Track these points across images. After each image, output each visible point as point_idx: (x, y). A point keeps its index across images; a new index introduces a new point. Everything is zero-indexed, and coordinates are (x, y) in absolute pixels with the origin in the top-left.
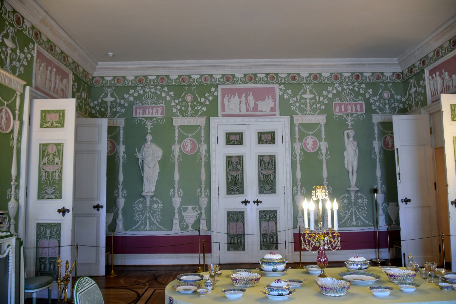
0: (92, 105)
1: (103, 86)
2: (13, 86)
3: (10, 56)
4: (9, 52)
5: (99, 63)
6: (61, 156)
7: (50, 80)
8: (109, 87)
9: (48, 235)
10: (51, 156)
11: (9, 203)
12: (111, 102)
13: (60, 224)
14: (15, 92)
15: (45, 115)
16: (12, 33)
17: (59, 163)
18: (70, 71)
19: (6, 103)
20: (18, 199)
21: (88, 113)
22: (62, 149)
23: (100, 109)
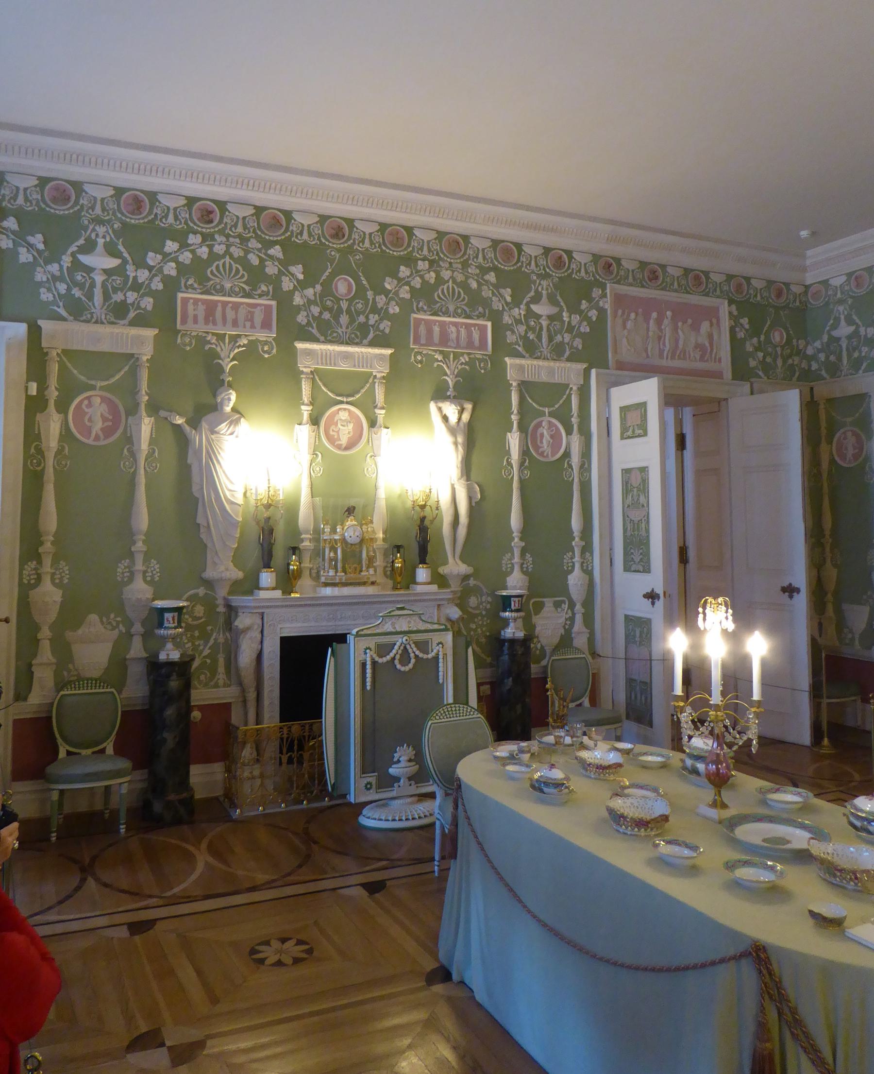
0: (810, 351)
1: (827, 304)
2: (557, 379)
3: (548, 330)
4: (545, 323)
5: (809, 253)
7: (659, 338)
8: (841, 302)
10: (635, 490)
12: (849, 337)
16: (547, 289)
18: (719, 300)
19: (547, 410)
21: (797, 374)
23: (827, 357)
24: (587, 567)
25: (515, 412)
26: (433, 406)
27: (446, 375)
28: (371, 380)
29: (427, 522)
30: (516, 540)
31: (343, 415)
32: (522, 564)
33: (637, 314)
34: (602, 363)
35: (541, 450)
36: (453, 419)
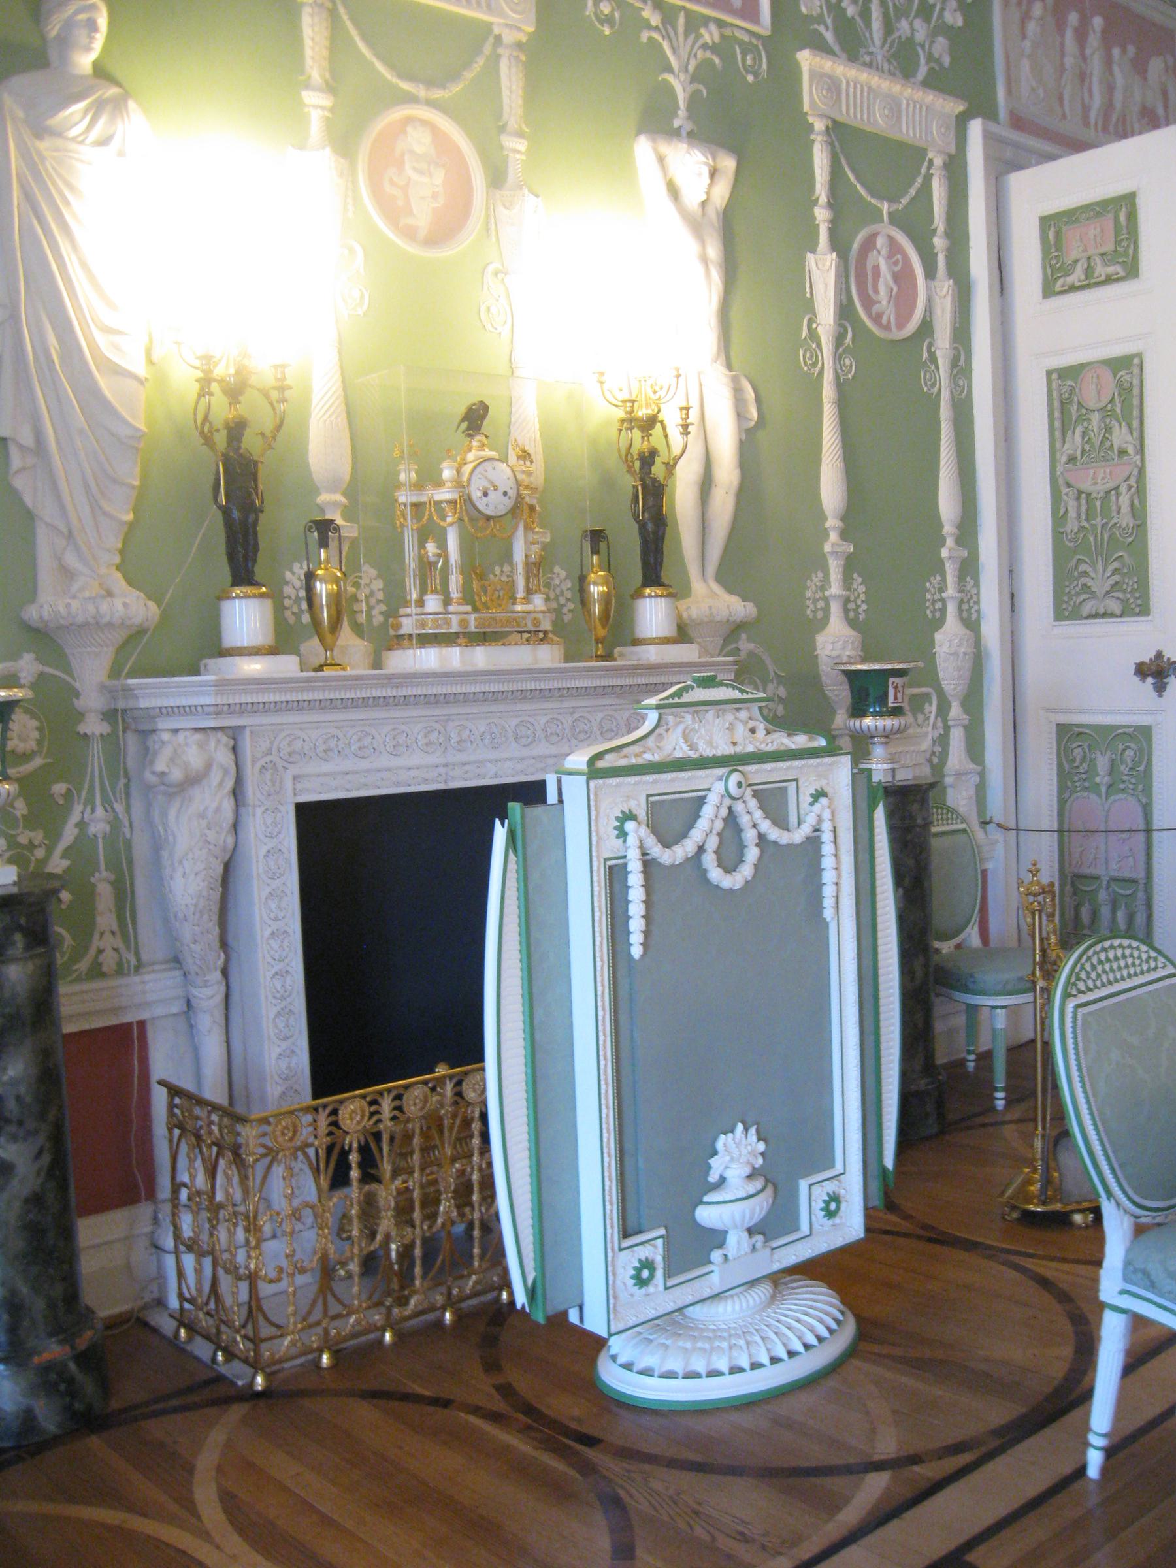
2: (907, 131)
6: (1135, 413)
7: (1083, 77)
9: (1102, 779)
10: (1095, 418)
11: (938, 636)
13: (1145, 733)
14: (922, 152)
15: (1058, 234)
17: (1131, 450)
19: (885, 207)
20: (978, 621)
22: (1136, 382)
24: (970, 614)
25: (823, 199)
26: (643, 148)
27: (669, 69)
28: (487, 48)
29: (658, 470)
30: (833, 537)
31: (418, 141)
32: (847, 601)
33: (1045, 9)
34: (988, 112)
35: (876, 309)
36: (694, 194)
